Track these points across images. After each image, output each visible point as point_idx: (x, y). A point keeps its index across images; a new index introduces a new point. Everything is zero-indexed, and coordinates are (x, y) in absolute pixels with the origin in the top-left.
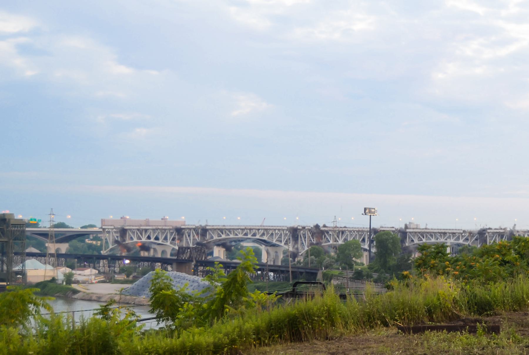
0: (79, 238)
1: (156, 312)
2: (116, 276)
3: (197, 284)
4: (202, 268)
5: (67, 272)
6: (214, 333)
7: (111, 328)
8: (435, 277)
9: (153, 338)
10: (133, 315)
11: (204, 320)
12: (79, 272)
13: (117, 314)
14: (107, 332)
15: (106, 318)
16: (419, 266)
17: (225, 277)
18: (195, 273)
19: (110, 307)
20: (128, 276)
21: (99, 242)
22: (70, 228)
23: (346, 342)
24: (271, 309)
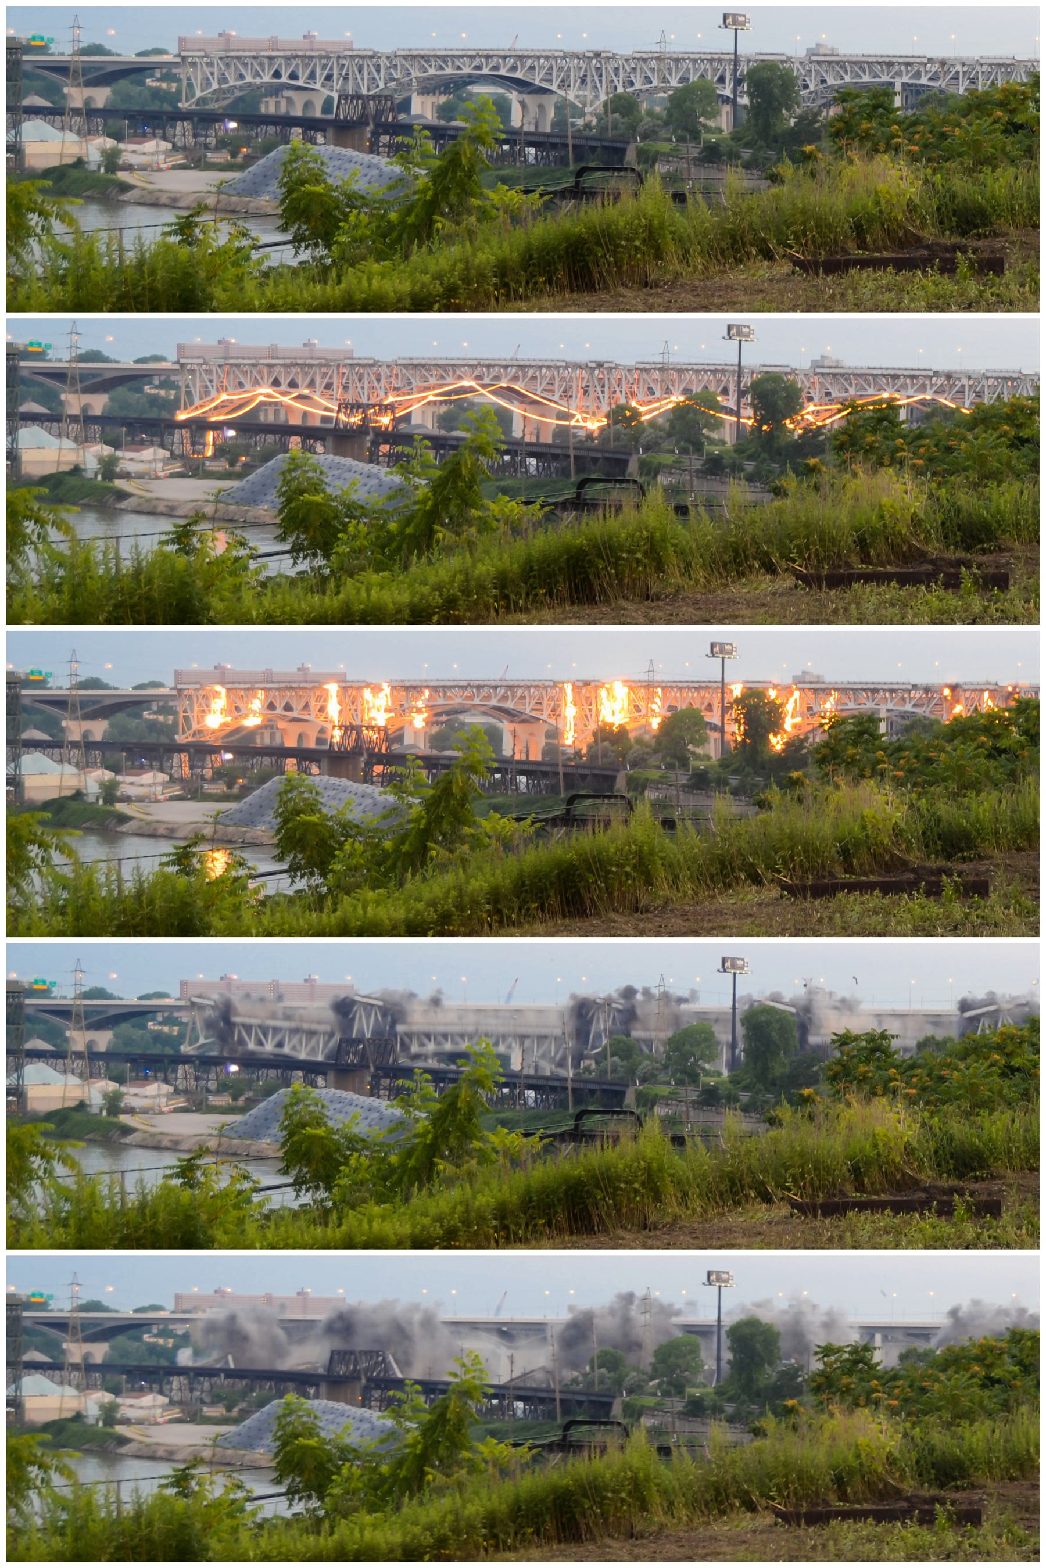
0: (134, 1020)
1: (294, 1173)
2: (211, 1098)
3: (377, 1115)
4: (388, 1081)
5: (110, 1089)
6: (412, 1216)
7: (200, 1206)
8: (869, 1101)
9: (286, 1226)
10: (245, 1177)
11: (391, 1190)
12: (133, 1090)
13: (214, 1178)
14: (192, 1213)
15: (190, 1183)
16: (834, 1078)
17: (434, 1100)
18: (374, 1092)
19: (198, 1162)
20: (235, 1098)
21: (176, 1028)
22: (115, 998)
23: (685, 1234)
24: (530, 1167)
